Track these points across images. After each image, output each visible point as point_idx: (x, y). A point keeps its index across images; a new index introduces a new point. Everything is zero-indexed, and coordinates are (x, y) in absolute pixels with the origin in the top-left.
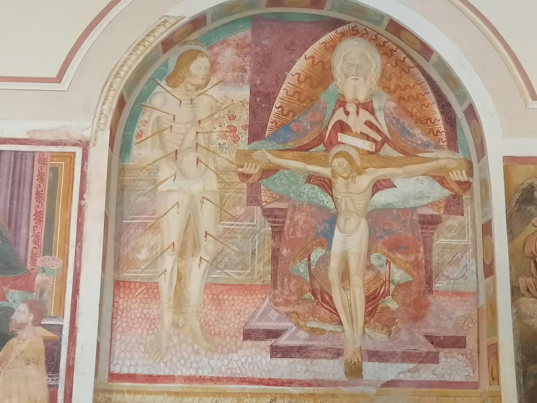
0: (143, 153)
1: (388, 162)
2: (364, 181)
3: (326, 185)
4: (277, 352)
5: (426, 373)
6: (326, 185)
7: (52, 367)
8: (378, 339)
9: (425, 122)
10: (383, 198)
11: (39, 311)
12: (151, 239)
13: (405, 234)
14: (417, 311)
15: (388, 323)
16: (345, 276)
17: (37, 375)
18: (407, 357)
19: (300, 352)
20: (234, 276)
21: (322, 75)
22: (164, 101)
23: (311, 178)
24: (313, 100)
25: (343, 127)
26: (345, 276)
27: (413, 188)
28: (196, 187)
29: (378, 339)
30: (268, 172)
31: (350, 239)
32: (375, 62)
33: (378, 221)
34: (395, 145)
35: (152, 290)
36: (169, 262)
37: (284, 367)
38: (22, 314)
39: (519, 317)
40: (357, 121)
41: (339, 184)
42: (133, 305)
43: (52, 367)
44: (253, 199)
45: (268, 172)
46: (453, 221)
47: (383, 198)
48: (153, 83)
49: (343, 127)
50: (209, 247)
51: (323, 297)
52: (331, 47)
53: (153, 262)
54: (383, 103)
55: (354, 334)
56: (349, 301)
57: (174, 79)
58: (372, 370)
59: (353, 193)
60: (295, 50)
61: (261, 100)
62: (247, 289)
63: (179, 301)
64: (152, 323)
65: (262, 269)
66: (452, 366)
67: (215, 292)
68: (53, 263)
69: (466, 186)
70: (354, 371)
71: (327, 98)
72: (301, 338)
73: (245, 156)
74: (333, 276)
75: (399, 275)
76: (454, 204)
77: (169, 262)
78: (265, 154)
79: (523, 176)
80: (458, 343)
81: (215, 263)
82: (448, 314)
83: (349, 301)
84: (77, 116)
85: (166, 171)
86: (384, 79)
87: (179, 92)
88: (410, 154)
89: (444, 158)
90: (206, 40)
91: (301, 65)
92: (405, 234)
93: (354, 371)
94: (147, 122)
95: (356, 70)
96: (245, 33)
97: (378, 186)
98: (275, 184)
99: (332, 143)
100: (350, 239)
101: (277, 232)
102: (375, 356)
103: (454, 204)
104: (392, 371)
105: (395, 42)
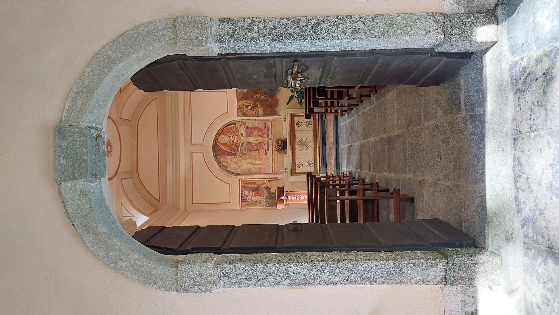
0: (239, 171)
1: (238, 134)
2: (242, 138)
3: (243, 143)
4: (268, 150)
5: (270, 128)
6: (243, 143)
7: (272, 180)
8: (265, 135)
9: (231, 128)
10: (244, 135)
11: (264, 183)
12: (252, 169)
13: (250, 132)
14: (261, 130)
15: (263, 134)
16: (257, 140)
17: (272, 182)
18: (268, 131)
19: (268, 147)
20: (257, 157)
21: (225, 145)
22: (230, 169)
23: (242, 146)
24: (229, 146)
25: (233, 141)
26: (257, 140)
27: (242, 130)
28: (244, 163)
29: (265, 135)
30: (241, 152)
31: (251, 140)
32: (222, 136)
33: (248, 136)
34: (235, 133)
35: (260, 168)
36: (256, 166)
37: (270, 149)
38: (265, 185)
39: (261, 116)
40: (232, 139)
41: (242, 142)
42: (262, 171)
43: (272, 180)
44: (246, 154)
45: (241, 152)
46: (247, 124)
47: (244, 135)
48: (228, 171)
49: (233, 141)
50: (253, 161)
51: (260, 144)
52: (220, 143)
53: (256, 168)
54: (229, 135)
55: (265, 139)
56: (260, 139)
57: (227, 168)
58: (270, 137)
59: (244, 139)
60: (221, 149)
61: (229, 154)
62: (259, 154)
63: (261, 164)
64: (265, 168)
65: (256, 152)
66: (269, 125)
67: (260, 159)
68: (257, 182)
69: (241, 122)
70: (270, 139)
71: (229, 144)
72: (266, 146)
73: (239, 156)
74: (257, 142)
75: (256, 132)
76: (245, 124)
77: (256, 166)
78: (238, 153)
79: (240, 114)
80: (265, 124)
81: (256, 160)
82: (261, 125)
83: (260, 139)
84: (235, 181)
85: (242, 168)
86: (224, 135)
87: (229, 167)
88: (237, 131)
89: (237, 125)
90: (220, 163)
91: (223, 148)
92: (250, 132)
93: (270, 139)
94: (234, 171)
95: (223, 139)
96: (218, 157)
97: (242, 136)
98: (243, 151)
99: (236, 143)
100: (251, 140)
101: (250, 151)
102: (268, 136)
103: (245, 124)
104: (270, 133)
105: (219, 134)
